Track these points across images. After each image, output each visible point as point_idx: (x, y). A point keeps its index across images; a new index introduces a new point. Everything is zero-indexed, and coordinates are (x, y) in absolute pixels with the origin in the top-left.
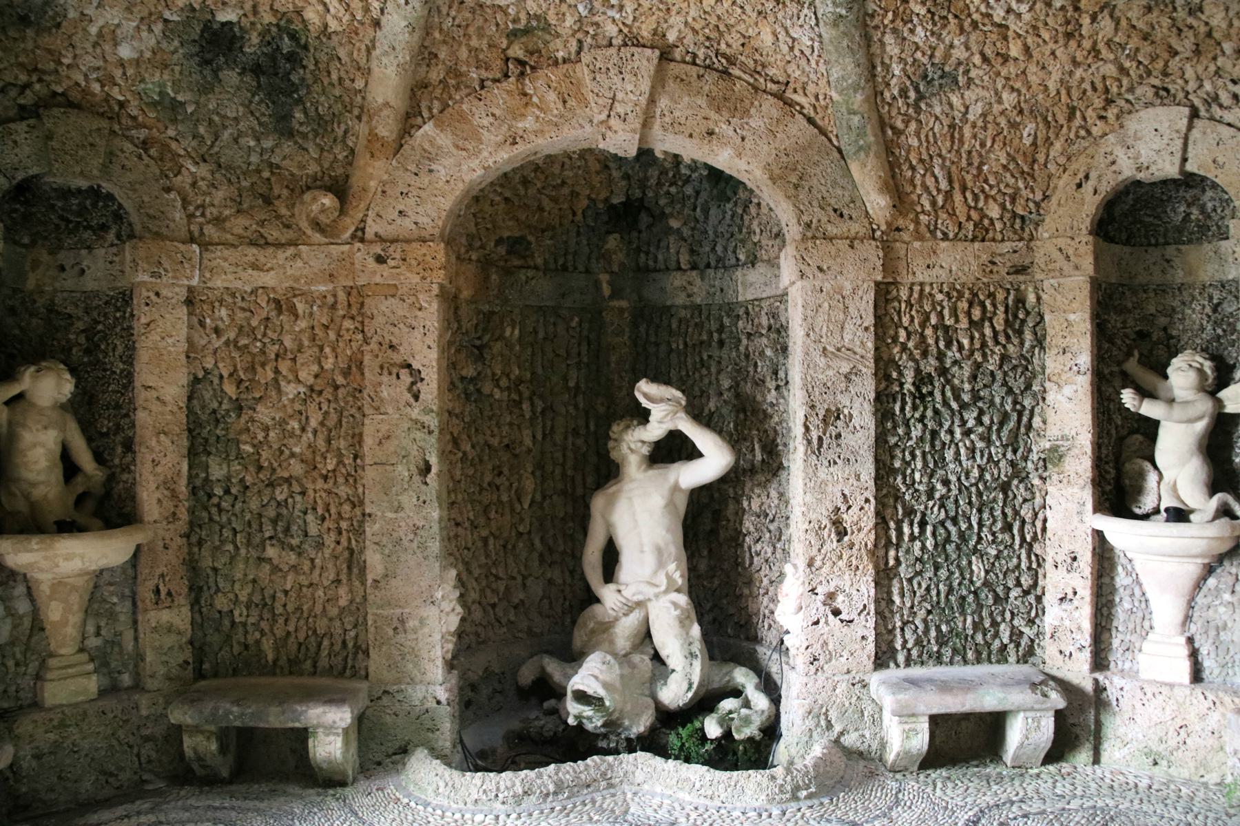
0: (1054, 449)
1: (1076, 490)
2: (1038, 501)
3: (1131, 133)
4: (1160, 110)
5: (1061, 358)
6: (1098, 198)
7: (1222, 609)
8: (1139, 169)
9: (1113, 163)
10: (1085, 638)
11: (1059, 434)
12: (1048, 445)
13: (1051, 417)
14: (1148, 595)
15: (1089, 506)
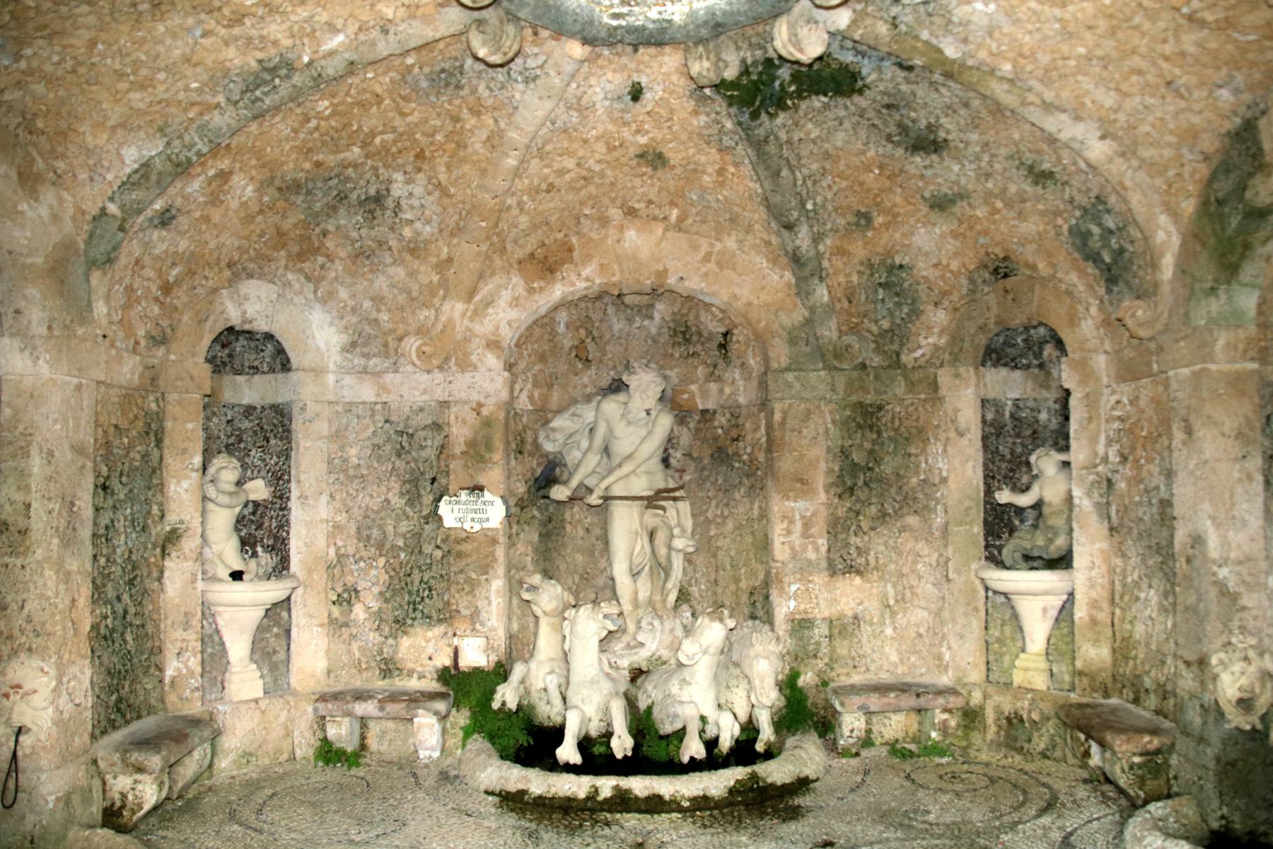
0: (174, 531)
1: (190, 563)
2: (155, 574)
3: (242, 292)
4: (260, 283)
5: (179, 458)
6: (213, 336)
7: (272, 640)
8: (244, 322)
9: (223, 312)
10: (196, 682)
11: (178, 519)
12: (168, 529)
13: (172, 506)
14: (225, 638)
15: (200, 576)
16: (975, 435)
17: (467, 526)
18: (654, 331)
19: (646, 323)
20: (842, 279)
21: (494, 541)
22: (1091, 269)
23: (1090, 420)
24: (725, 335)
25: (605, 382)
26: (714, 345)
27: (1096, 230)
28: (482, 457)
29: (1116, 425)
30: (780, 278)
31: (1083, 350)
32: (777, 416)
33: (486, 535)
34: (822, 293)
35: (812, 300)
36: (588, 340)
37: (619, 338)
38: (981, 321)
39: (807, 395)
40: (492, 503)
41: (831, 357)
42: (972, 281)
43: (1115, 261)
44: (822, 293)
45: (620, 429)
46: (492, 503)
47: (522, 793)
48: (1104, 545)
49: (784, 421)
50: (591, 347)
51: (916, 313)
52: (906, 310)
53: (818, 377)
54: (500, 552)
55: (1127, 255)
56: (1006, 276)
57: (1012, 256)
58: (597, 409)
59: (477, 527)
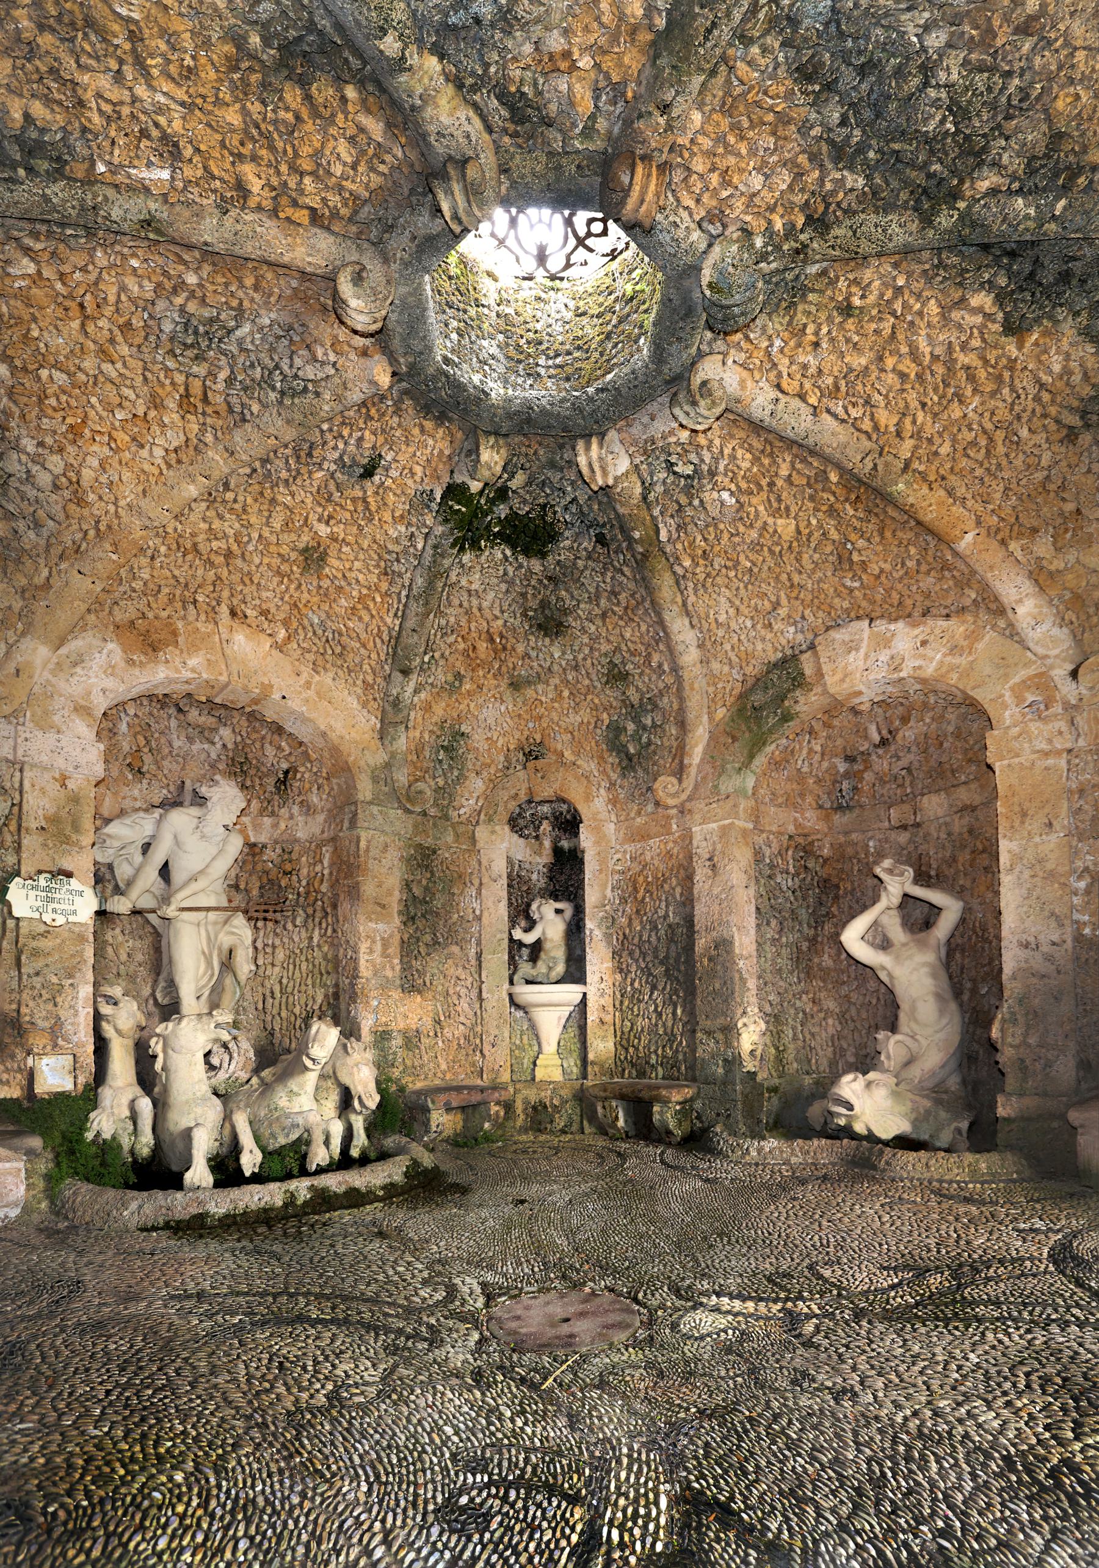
16: (504, 881)
17: (47, 918)
18: (214, 756)
19: (206, 746)
20: (418, 734)
21: (81, 938)
22: (613, 759)
23: (601, 871)
24: (286, 773)
25: (157, 801)
26: (271, 781)
27: (631, 727)
28: (68, 838)
29: (616, 877)
30: (366, 723)
31: (595, 819)
32: (363, 844)
33: (70, 931)
34: (402, 743)
35: (395, 746)
36: (146, 750)
37: (178, 755)
38: (513, 792)
39: (387, 828)
40: (81, 894)
41: (405, 799)
42: (507, 759)
43: (639, 754)
44: (402, 743)
45: (191, 842)
46: (81, 894)
47: (201, 1217)
48: (610, 964)
49: (367, 850)
50: (148, 759)
51: (461, 779)
52: (456, 773)
53: (395, 813)
54: (89, 952)
55: (653, 747)
56: (536, 758)
57: (546, 742)
58: (159, 822)
59: (60, 920)
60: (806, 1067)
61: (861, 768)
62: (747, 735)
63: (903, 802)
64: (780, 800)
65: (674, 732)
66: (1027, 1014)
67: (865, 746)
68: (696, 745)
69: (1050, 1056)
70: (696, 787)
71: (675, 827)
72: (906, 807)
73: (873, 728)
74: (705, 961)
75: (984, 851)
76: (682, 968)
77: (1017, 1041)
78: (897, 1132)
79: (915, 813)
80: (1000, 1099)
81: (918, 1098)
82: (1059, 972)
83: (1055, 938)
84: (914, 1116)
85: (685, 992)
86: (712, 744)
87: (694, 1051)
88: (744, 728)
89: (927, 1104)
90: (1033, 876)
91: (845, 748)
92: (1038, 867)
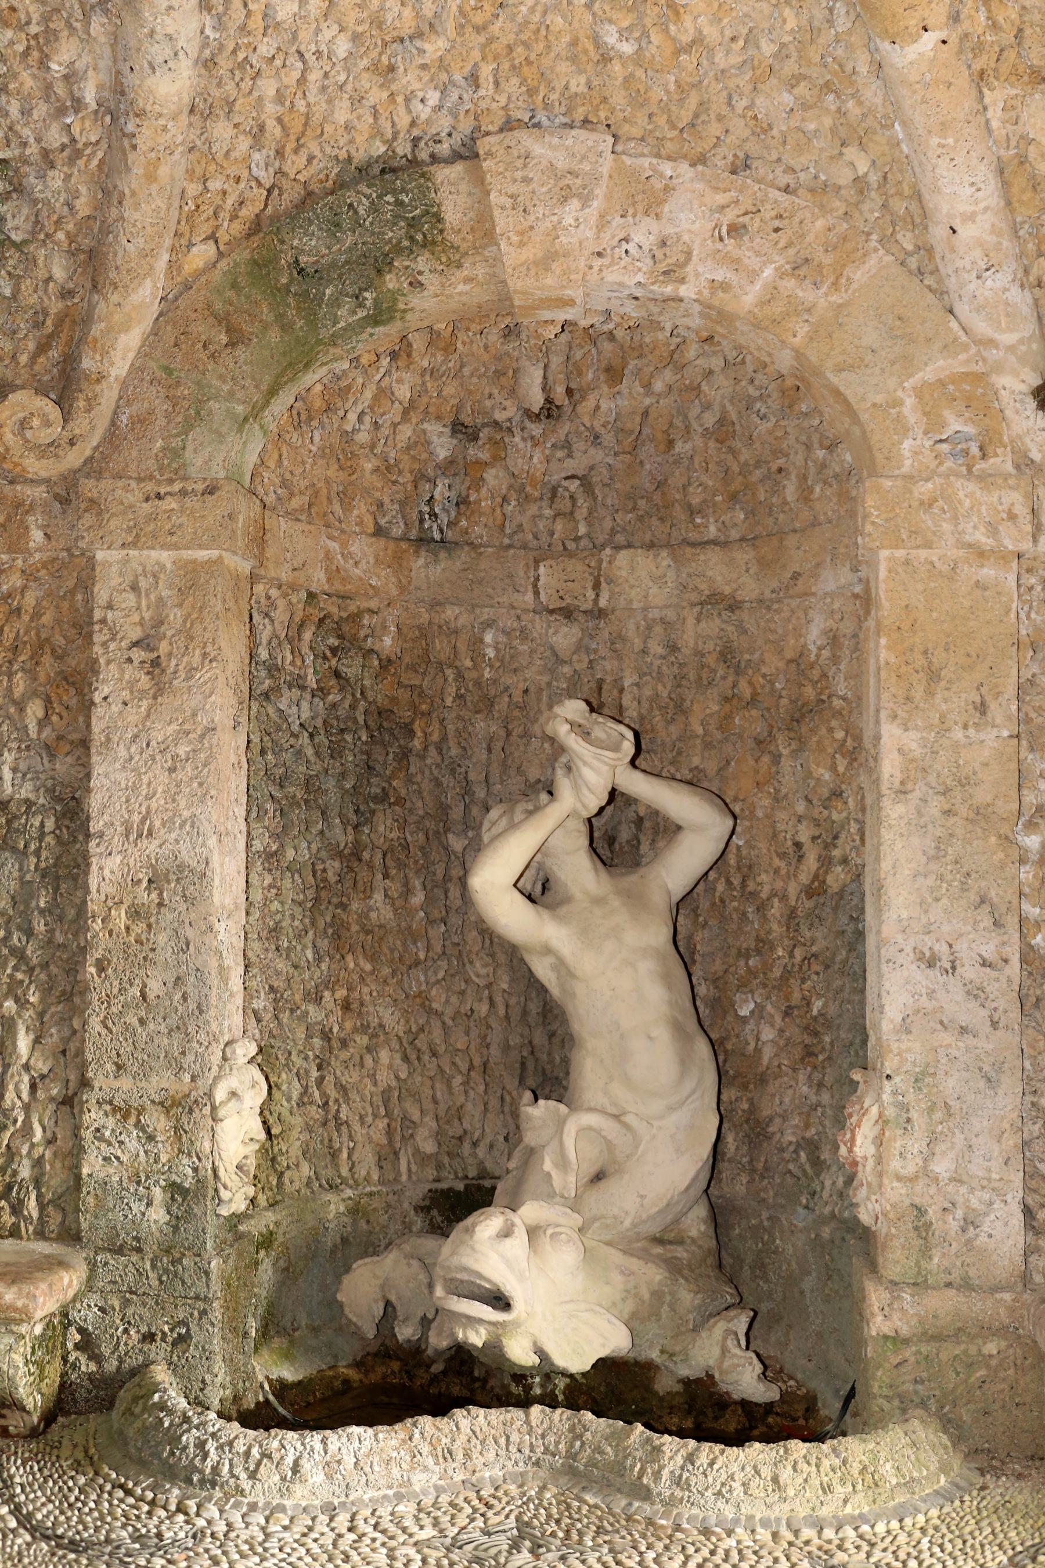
60: (327, 1173)
61: (484, 456)
62: (274, 336)
63: (571, 555)
64: (296, 503)
65: (59, 273)
66: (931, 1110)
67: (507, 412)
68: (125, 327)
69: (974, 1203)
70: (113, 436)
71: (37, 536)
72: (576, 568)
73: (536, 375)
74: (120, 918)
75: (753, 701)
76: (40, 926)
77: (910, 1168)
78: (603, 1354)
79: (597, 586)
80: (876, 1297)
81: (634, 1264)
82: (995, 1025)
83: (989, 951)
84: (629, 1306)
85: (46, 991)
86: (169, 334)
87: (75, 1154)
88: (266, 313)
89: (654, 1275)
90: (948, 813)
91: (459, 408)
92: (958, 794)
